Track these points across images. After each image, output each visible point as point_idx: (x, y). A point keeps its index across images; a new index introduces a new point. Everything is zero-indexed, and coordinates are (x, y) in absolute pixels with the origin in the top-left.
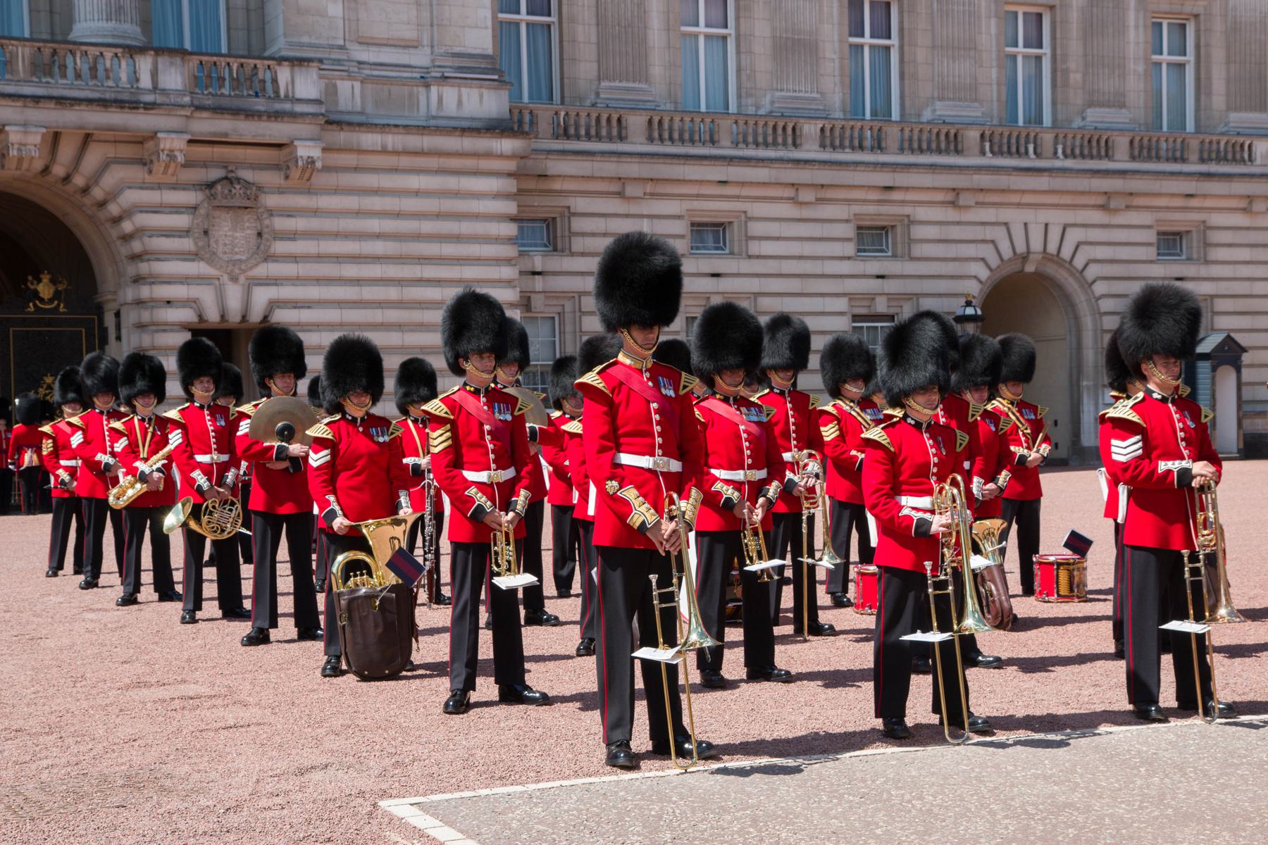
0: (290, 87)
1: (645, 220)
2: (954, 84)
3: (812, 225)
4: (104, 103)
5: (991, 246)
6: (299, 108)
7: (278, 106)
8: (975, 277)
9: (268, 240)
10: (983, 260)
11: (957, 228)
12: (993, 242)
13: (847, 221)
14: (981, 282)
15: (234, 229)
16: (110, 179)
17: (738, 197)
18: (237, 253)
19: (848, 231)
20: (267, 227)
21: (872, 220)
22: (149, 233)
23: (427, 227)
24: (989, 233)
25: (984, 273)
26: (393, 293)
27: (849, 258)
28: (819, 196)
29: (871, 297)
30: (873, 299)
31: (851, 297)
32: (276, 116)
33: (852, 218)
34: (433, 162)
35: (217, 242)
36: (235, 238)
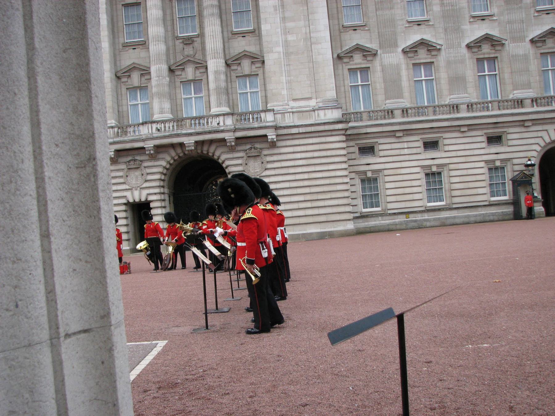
0: (265, 118)
1: (405, 143)
2: (521, 84)
3: (468, 138)
4: (210, 132)
5: (541, 139)
6: (268, 124)
7: (261, 125)
8: (535, 150)
9: (265, 164)
10: (537, 144)
11: (526, 134)
12: (541, 137)
13: (482, 135)
14: (537, 152)
15: (254, 162)
16: (217, 154)
17: (439, 132)
18: (256, 170)
19: (484, 139)
20: (265, 160)
21: (491, 134)
22: (230, 167)
23: (316, 154)
24: (540, 134)
25: (538, 148)
26: (306, 176)
27: (484, 148)
28: (469, 128)
29: (494, 161)
30: (495, 161)
31: (486, 162)
32: (261, 128)
33: (483, 134)
34: (317, 135)
35: (249, 167)
36: (255, 165)
